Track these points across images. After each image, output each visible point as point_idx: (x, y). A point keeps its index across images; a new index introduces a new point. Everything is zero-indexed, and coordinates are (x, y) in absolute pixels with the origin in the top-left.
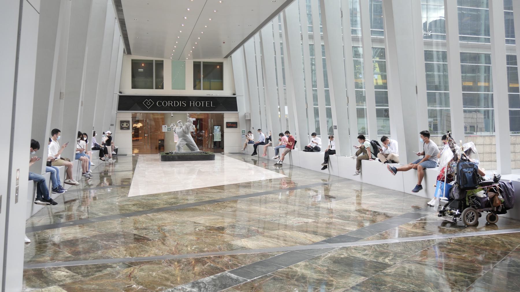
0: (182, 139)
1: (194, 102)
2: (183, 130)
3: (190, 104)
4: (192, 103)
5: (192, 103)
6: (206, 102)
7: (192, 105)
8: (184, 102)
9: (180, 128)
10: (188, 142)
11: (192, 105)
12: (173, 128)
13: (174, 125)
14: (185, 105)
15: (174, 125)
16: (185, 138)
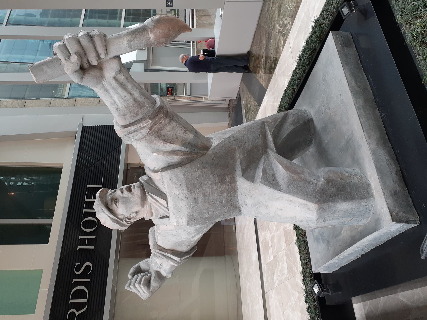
0: (252, 179)
1: (81, 237)
2: (170, 167)
3: (86, 247)
4: (83, 242)
5: (83, 242)
6: (86, 200)
7: (90, 242)
8: (78, 269)
9: (163, 196)
10: (266, 146)
11: (90, 242)
12: (159, 275)
13: (139, 271)
14: (88, 266)
15: (139, 271)
16: (239, 156)
